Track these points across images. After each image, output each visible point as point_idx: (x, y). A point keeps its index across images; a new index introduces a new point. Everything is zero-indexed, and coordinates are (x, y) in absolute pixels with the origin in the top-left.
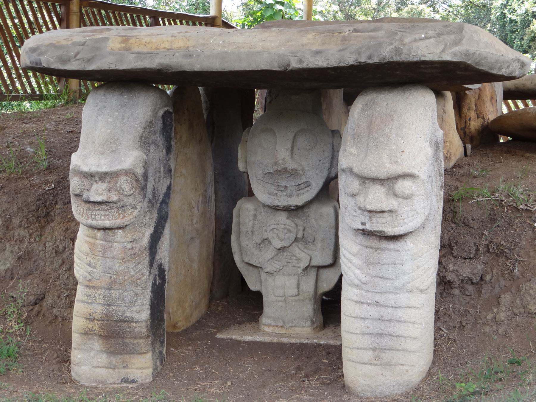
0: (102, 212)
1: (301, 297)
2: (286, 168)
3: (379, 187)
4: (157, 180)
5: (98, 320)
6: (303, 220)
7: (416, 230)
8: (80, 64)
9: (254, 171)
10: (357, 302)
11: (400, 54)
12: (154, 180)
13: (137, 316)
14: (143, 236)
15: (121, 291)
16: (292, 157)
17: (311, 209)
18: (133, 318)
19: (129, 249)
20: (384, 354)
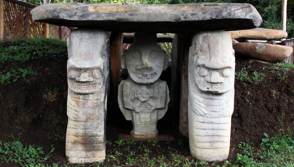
0: (85, 86)
1: (152, 122)
2: (147, 67)
3: (216, 72)
5: (81, 136)
6: (152, 89)
8: (78, 18)
9: (131, 69)
10: (202, 122)
11: (230, 16)
13: (99, 133)
14: (101, 97)
15: (91, 123)
17: (155, 84)
18: (97, 135)
19: (95, 103)
20: (214, 144)
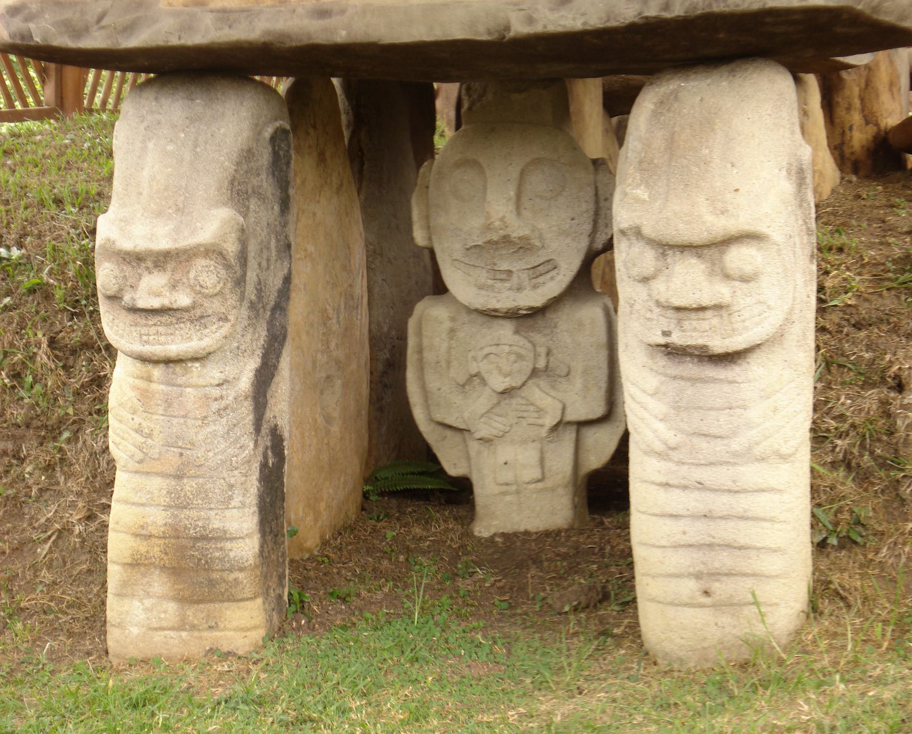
1: (549, 483)
3: (694, 261)
4: (264, 264)
7: (767, 341)
9: (446, 245)
12: (259, 264)
15: (201, 481)
16: (519, 214)
17: (560, 313)
18: (225, 532)
20: (717, 584)
